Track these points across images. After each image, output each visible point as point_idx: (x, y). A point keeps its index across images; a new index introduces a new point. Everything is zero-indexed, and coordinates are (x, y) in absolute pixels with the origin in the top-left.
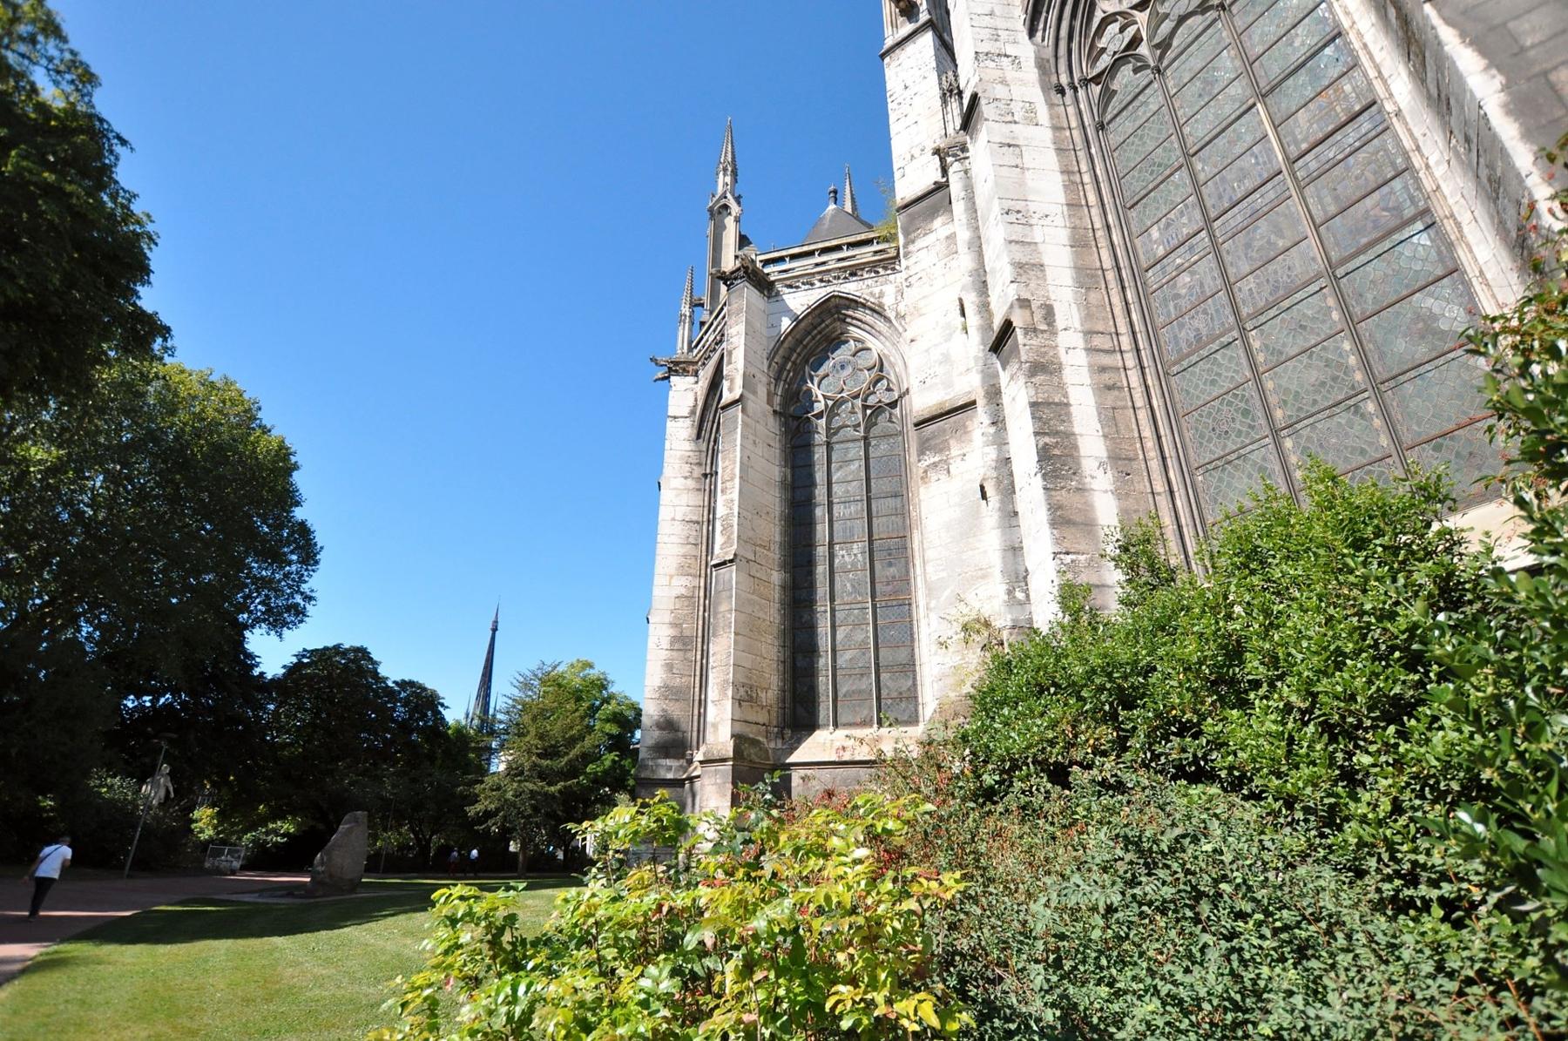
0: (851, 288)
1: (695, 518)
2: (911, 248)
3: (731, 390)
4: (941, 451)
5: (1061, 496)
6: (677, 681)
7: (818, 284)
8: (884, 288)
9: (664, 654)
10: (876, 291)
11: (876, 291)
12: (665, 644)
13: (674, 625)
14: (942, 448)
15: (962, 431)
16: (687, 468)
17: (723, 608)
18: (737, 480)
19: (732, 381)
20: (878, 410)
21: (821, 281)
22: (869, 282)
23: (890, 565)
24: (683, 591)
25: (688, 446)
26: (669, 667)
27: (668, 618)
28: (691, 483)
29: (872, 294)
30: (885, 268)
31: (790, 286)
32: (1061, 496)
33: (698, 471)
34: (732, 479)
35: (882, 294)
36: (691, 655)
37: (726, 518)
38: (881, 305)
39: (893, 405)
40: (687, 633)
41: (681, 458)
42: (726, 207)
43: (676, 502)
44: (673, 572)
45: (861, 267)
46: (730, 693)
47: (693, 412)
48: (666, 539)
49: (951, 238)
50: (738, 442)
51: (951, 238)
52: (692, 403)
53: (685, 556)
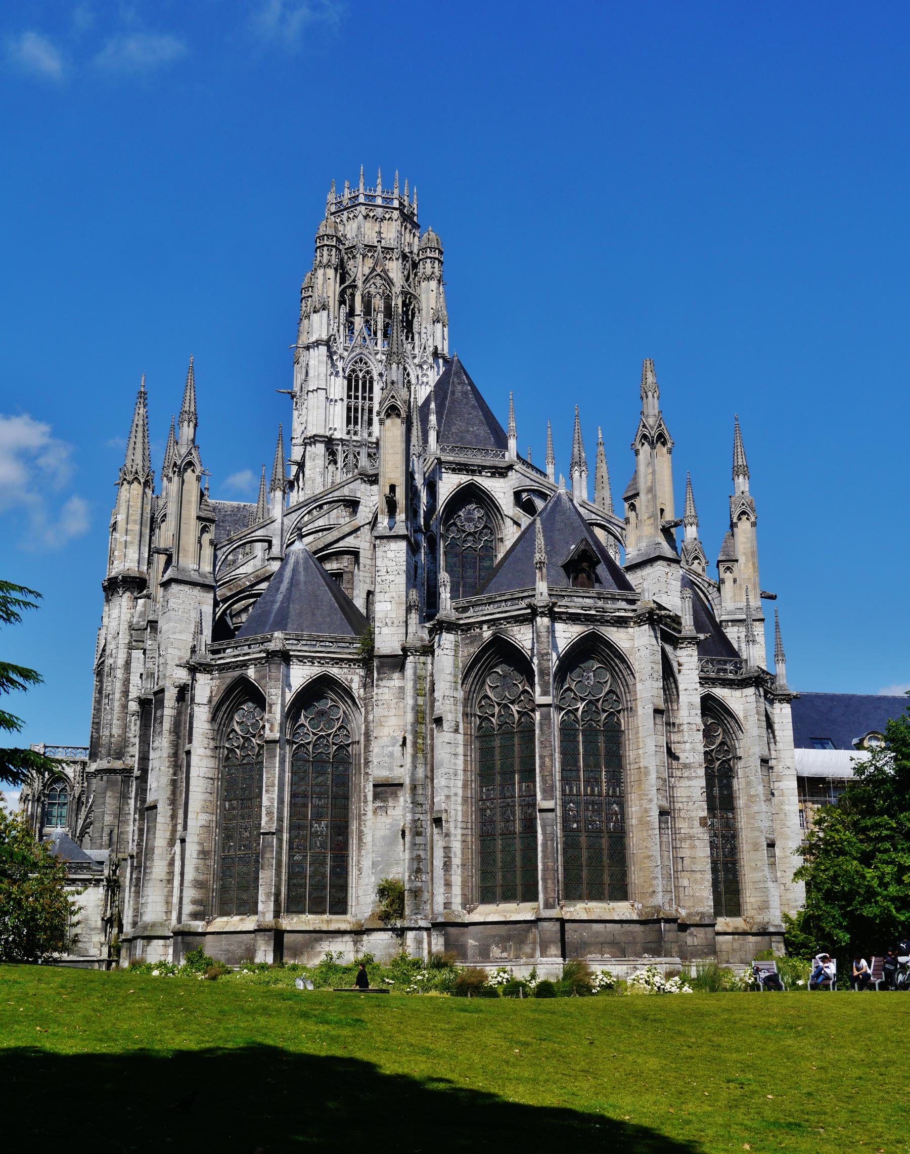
0: (335, 671)
1: (210, 776)
2: (380, 683)
3: (271, 730)
4: (384, 801)
5: (447, 877)
6: (201, 877)
7: (316, 664)
8: (353, 677)
9: (194, 861)
10: (349, 677)
11: (349, 677)
12: (195, 855)
13: (200, 844)
14: (385, 800)
15: (395, 795)
16: (206, 741)
17: (268, 855)
18: (276, 788)
19: (272, 725)
20: (341, 747)
21: (319, 662)
22: (345, 670)
23: (339, 835)
24: (204, 823)
25: (207, 726)
26: (197, 869)
27: (196, 839)
28: (209, 753)
29: (347, 680)
30: (355, 665)
31: (301, 661)
32: (447, 877)
33: (212, 744)
34: (273, 786)
35: (352, 680)
36: (207, 862)
37: (268, 808)
38: (351, 688)
39: (348, 745)
40: (206, 849)
41: (203, 734)
42: (190, 464)
43: (200, 764)
44: (199, 810)
45: (342, 660)
46: (273, 899)
47: (210, 702)
48: (194, 789)
49: (402, 689)
50: (277, 765)
51: (402, 689)
52: (208, 694)
53: (205, 801)
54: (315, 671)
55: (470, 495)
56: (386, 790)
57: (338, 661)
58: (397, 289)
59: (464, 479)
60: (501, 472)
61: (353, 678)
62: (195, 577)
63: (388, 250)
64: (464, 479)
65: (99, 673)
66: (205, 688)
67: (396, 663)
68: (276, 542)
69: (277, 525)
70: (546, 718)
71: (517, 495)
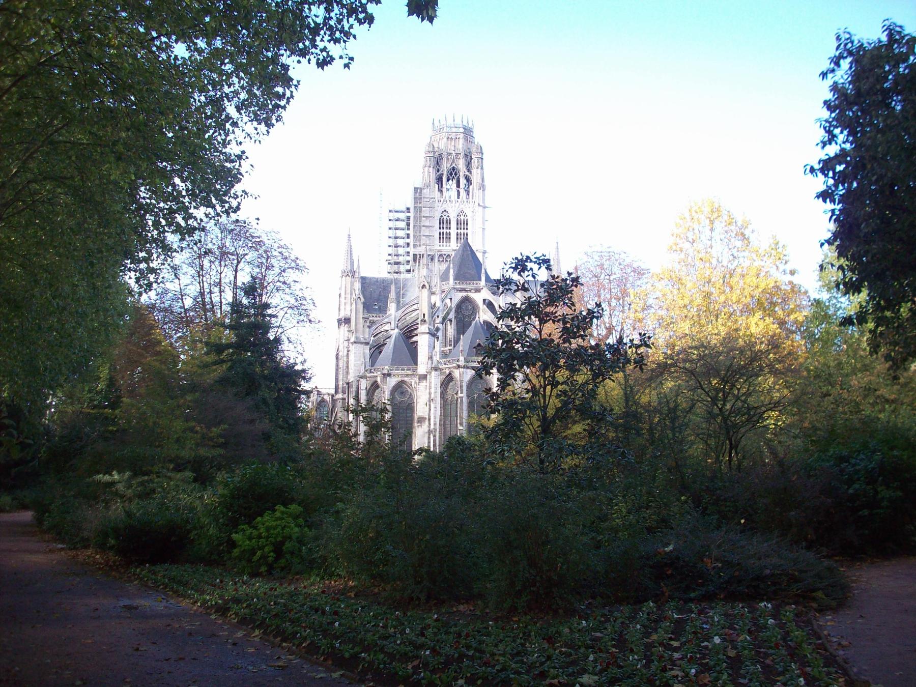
0: (406, 379)
54: (400, 379)
55: (466, 300)
56: (421, 420)
57: (407, 375)
58: (462, 174)
59: (464, 294)
60: (478, 290)
61: (414, 381)
62: (362, 340)
63: (457, 154)
64: (464, 294)
65: (337, 358)
66: (364, 384)
67: (424, 377)
68: (393, 323)
69: (393, 316)
70: (462, 401)
71: (484, 300)
